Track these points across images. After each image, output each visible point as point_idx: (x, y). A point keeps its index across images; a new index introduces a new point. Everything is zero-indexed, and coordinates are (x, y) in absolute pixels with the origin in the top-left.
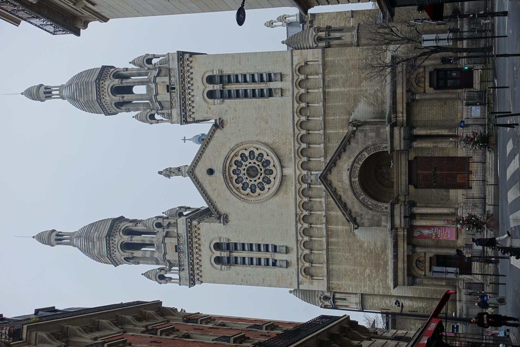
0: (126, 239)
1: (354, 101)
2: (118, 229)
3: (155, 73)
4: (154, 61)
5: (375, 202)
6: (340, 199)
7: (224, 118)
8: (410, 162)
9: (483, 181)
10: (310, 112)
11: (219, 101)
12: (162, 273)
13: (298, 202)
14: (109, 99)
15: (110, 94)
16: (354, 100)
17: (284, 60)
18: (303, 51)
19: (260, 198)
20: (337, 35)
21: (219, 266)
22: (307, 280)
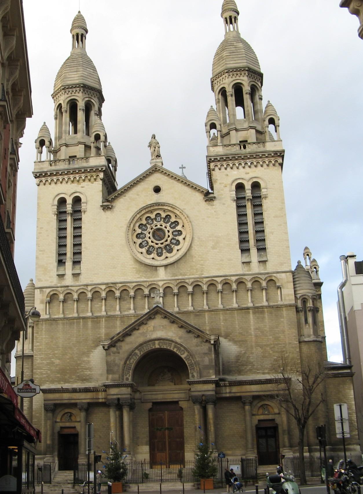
0: (81, 105)
1: (239, 341)
3: (259, 128)
4: (271, 127)
5: (133, 366)
6: (134, 329)
7: (215, 202)
8: (177, 403)
9: (162, 480)
10: (226, 294)
11: (234, 195)
12: (47, 143)
13: (128, 284)
14: (228, 83)
16: (242, 341)
17: (282, 264)
18: (292, 284)
19: (132, 243)
20: (310, 320)
21: (56, 203)
22: (45, 297)
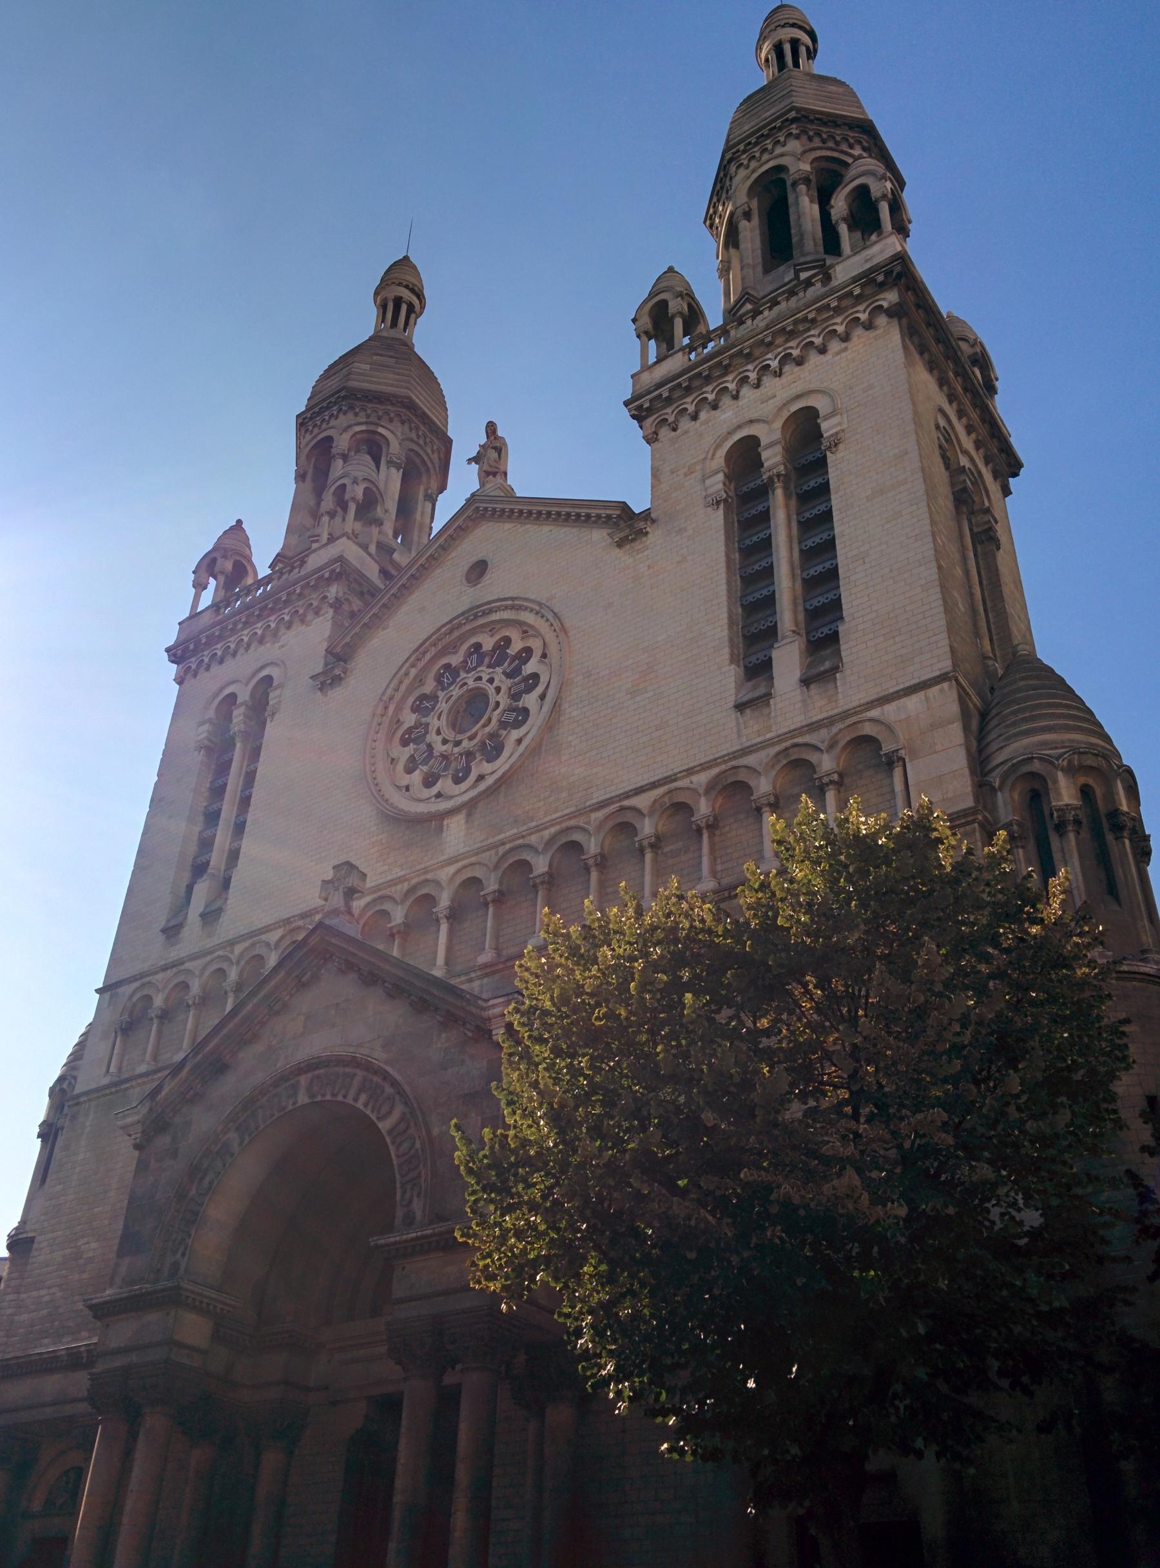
2: (379, 418)
15: (755, 175)
